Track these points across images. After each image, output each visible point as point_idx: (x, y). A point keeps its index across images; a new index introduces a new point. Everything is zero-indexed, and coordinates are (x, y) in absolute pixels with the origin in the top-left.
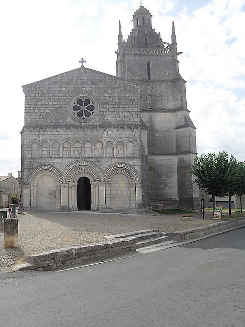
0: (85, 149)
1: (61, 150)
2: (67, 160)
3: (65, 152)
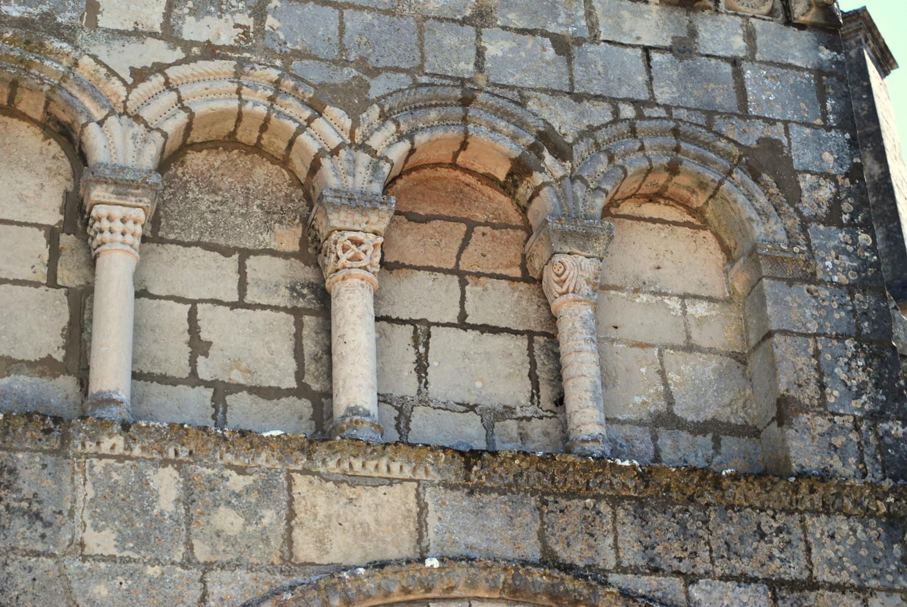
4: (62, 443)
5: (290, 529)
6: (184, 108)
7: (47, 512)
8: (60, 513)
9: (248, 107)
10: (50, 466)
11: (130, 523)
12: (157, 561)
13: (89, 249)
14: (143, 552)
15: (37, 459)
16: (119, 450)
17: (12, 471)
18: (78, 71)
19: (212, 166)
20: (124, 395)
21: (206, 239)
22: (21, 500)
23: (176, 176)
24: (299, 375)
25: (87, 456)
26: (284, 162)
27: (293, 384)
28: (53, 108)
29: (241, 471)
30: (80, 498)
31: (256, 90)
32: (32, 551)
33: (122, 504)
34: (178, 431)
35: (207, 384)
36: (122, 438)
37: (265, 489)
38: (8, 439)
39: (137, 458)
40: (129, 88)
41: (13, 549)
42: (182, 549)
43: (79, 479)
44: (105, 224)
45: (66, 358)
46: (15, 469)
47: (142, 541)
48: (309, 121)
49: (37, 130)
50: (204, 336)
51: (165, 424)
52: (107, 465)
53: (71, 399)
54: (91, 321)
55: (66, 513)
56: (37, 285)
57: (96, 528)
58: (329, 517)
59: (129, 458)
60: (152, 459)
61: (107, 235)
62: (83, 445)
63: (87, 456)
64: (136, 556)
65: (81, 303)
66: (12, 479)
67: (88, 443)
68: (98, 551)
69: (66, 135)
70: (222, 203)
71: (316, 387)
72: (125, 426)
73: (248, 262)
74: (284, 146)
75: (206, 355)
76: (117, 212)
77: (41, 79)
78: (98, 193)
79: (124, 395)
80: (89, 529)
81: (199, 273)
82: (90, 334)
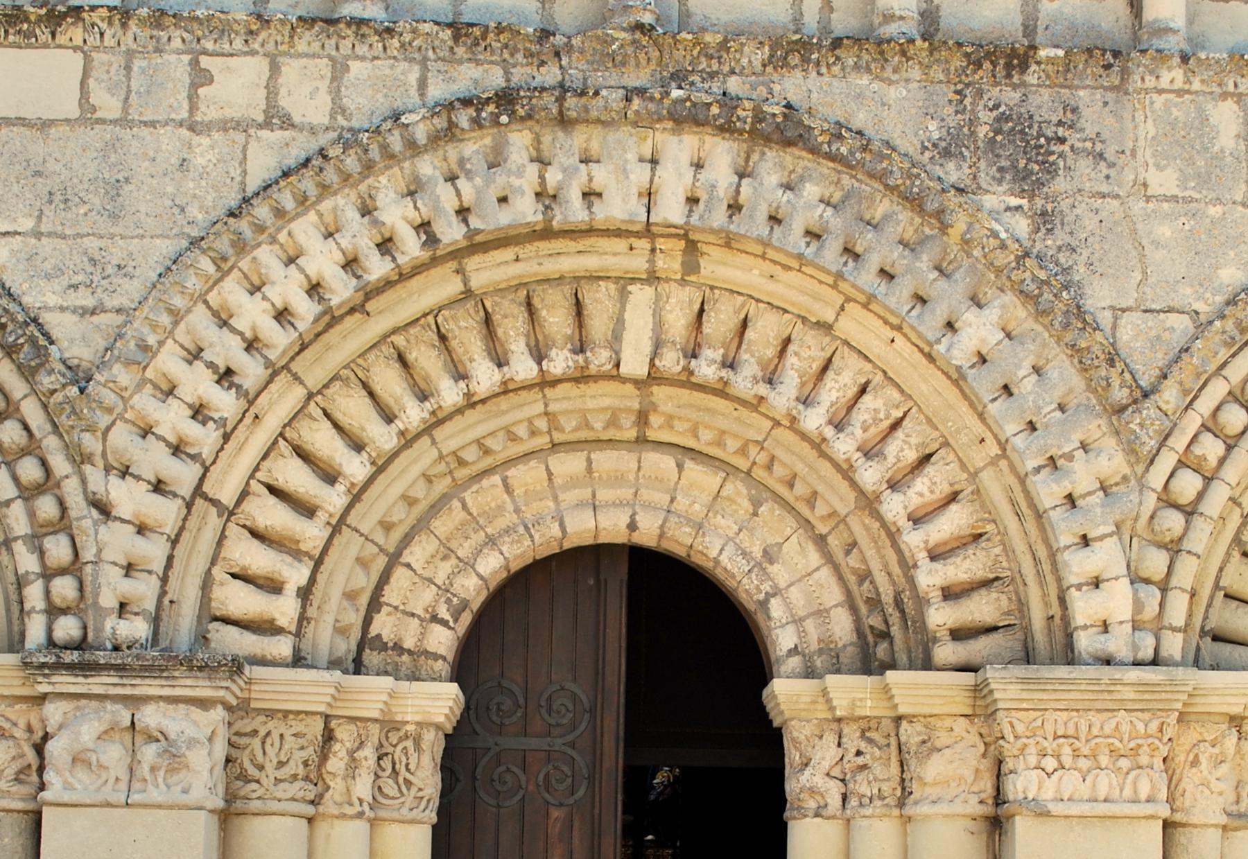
2: (237, 82)
4: (1122, 79)
7: (1110, 154)
8: (1123, 152)
10: (1111, 104)
11: (1190, 161)
12: (1219, 201)
14: (1204, 192)
15: (1099, 96)
16: (1179, 84)
17: (1074, 110)
20: (1179, 22)
22: (1085, 140)
25: (1147, 91)
32: (1098, 193)
33: (1183, 141)
36: (1181, 71)
38: (1069, 76)
39: (1197, 92)
41: (1079, 190)
43: (1139, 115)
46: (1078, 108)
47: (1204, 180)
51: (1225, 56)
52: (1166, 100)
55: (1128, 153)
57: (1158, 167)
59: (1188, 92)
60: (1212, 93)
62: (1143, 79)
63: (1147, 91)
64: (1197, 196)
66: (1075, 118)
67: (1147, 78)
68: (1161, 191)
72: (1185, 59)
79: (1179, 22)
80: (1152, 169)
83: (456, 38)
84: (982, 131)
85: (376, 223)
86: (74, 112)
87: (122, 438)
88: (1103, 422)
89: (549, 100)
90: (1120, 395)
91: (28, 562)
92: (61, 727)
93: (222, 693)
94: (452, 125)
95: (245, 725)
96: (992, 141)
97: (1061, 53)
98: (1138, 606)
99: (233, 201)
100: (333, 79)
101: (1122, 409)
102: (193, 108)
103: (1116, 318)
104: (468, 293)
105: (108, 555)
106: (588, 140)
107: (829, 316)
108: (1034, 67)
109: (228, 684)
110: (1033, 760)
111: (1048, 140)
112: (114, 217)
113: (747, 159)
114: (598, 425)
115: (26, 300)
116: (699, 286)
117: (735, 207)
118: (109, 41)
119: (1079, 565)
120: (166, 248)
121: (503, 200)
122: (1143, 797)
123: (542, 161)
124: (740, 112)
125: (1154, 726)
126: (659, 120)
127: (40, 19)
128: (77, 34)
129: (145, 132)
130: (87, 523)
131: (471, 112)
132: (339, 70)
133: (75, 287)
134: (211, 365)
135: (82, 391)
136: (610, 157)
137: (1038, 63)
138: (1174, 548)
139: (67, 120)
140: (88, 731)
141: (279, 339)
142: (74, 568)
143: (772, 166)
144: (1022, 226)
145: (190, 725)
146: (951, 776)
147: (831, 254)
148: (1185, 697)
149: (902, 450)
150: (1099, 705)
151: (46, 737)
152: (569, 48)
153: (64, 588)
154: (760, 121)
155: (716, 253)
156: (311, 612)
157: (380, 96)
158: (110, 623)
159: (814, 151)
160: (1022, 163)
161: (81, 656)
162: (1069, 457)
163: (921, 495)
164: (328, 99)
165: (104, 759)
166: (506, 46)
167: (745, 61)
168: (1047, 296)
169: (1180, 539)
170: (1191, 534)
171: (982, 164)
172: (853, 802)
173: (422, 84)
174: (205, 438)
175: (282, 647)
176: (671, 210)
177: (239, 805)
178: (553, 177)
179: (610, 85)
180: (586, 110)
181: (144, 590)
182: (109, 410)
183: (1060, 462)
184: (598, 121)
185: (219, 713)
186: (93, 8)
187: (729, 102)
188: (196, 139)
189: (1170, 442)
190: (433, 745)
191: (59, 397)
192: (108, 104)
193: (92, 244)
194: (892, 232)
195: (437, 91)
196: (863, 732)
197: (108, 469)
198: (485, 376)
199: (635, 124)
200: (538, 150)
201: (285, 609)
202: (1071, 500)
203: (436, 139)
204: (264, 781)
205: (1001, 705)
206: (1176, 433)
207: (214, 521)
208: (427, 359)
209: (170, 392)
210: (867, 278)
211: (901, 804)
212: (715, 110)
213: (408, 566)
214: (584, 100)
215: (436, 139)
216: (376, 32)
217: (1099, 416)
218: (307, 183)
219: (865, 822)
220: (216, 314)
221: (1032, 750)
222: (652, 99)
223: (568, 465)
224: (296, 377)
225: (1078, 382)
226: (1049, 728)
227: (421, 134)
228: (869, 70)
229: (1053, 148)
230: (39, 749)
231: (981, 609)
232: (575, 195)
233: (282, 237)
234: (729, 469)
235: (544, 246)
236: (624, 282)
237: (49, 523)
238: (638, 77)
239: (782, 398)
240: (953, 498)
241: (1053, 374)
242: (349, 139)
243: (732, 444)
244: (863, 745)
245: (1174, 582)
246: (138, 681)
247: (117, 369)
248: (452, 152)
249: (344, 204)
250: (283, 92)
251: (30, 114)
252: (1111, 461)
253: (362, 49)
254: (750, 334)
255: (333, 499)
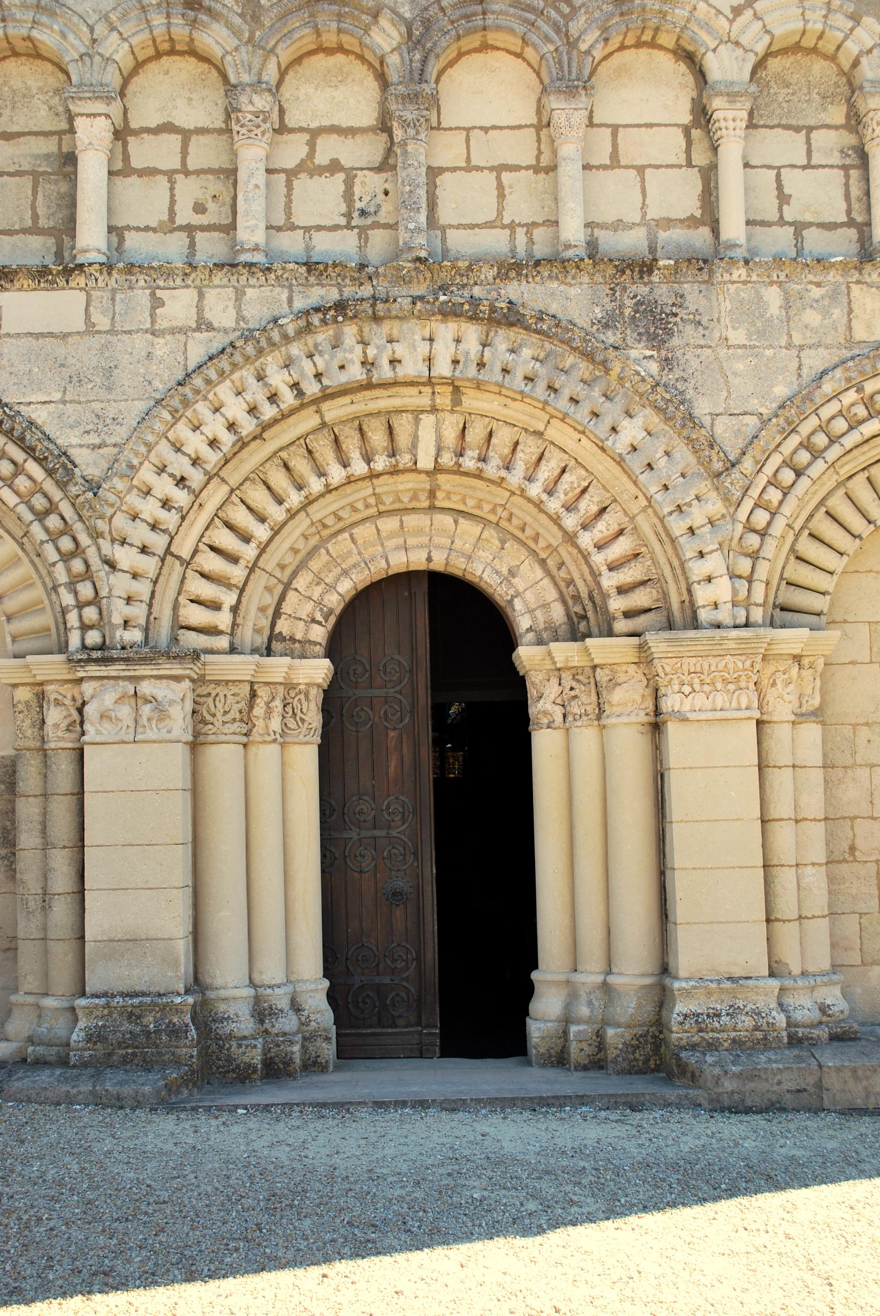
0: (448, 150)
1: (92, 169)
2: (179, 305)
3: (145, 202)
5: (850, 321)
6: (767, 32)
7: (704, 322)
9: (810, 26)
11: (753, 323)
13: (711, 139)
17: (682, 296)
18: (696, 14)
19: (785, 68)
20: (742, 241)
21: (784, 122)
23: (761, 78)
24: (849, 212)
26: (833, 58)
27: (845, 219)
28: (681, 42)
29: (818, 285)
30: (723, 309)
31: (815, 11)
34: (778, 260)
35: (790, 224)
37: (833, 296)
40: (731, 22)
42: (785, 337)
43: (721, 298)
44: (723, 124)
45: (702, 215)
47: (761, 334)
48: (852, 30)
49: (670, 56)
50: (787, 191)
53: (708, 242)
54: (717, 188)
56: (680, 167)
57: (734, 328)
58: (873, 311)
59: (749, 282)
61: (724, 131)
65: (709, 177)
69: (690, 59)
70: (793, 94)
71: (859, 219)
72: (747, 262)
73: (812, 136)
74: (833, 48)
75: (788, 204)
76: (730, 114)
77: (674, 23)
78: (717, 103)
79: (742, 241)
80: (730, 329)
81: (783, 147)
82: (717, 197)
83: (309, 271)
84: (627, 312)
85: (267, 385)
86: (82, 328)
87: (121, 522)
88: (708, 483)
89: (366, 306)
90: (718, 466)
91: (68, 599)
92: (92, 697)
93: (188, 672)
94: (309, 324)
95: (203, 690)
96: (634, 317)
97: (672, 262)
98: (735, 592)
99: (180, 376)
100: (237, 300)
101: (719, 474)
102: (153, 322)
103: (713, 420)
104: (324, 424)
105: (115, 592)
106: (391, 329)
107: (541, 427)
108: (656, 272)
109: (192, 666)
110: (676, 688)
111: (667, 315)
112: (109, 389)
113: (487, 336)
114: (406, 500)
115: (59, 442)
116: (462, 413)
117: (481, 365)
118: (101, 284)
119: (698, 569)
120: (141, 406)
121: (342, 367)
122: (744, 706)
123: (364, 343)
124: (481, 308)
125: (748, 664)
126: (433, 315)
127: (59, 272)
128: (81, 280)
129: (125, 337)
130: (102, 574)
131: (320, 315)
132: (240, 294)
133: (88, 432)
134: (172, 475)
135: (95, 494)
136: (405, 338)
137: (659, 269)
138: (755, 556)
139: (78, 333)
140: (109, 699)
141: (212, 458)
142: (96, 601)
143: (502, 339)
144: (654, 367)
145: (172, 693)
146: (628, 700)
147: (540, 390)
148: (765, 645)
149: (588, 505)
150: (715, 653)
151: (84, 704)
152: (377, 274)
153: (90, 613)
154: (494, 312)
155: (471, 393)
156: (239, 620)
157: (265, 309)
158: (119, 633)
159: (527, 328)
160: (652, 330)
161: (102, 654)
162: (689, 505)
163: (601, 532)
164: (234, 312)
165: (119, 715)
166: (339, 275)
167: (482, 277)
168: (671, 409)
169: (758, 551)
170: (764, 547)
171: (628, 332)
172: (570, 718)
173: (290, 300)
174: (170, 519)
175: (223, 642)
176: (443, 368)
177: (202, 738)
178: (371, 352)
179: (403, 294)
180: (389, 310)
181: (138, 612)
182: (112, 505)
183: (684, 508)
184: (397, 317)
185: (187, 684)
186: (90, 265)
187: (474, 301)
188: (156, 340)
189: (749, 493)
190: (316, 696)
191: (81, 499)
192: (102, 322)
193: (97, 406)
194: (576, 375)
195: (299, 304)
196: (574, 676)
197: (113, 541)
198: (337, 474)
199: (419, 318)
200: (361, 336)
201: (223, 620)
202: (691, 530)
203: (300, 333)
204: (216, 723)
205: (655, 656)
206: (753, 487)
207: (178, 568)
208: (301, 465)
209: (148, 492)
210: (563, 403)
211: (599, 718)
212: (466, 307)
213: (296, 590)
214: (387, 305)
215: (300, 333)
216: (261, 270)
217: (705, 479)
218: (224, 363)
219: (578, 730)
220: (173, 444)
221: (676, 681)
222: (428, 302)
223: (389, 524)
224: (223, 480)
225: (692, 459)
226: (685, 669)
227: (291, 330)
228: (557, 278)
229: (670, 320)
230: (80, 711)
231: (641, 598)
232: (385, 362)
233: (211, 396)
234: (486, 522)
235: (368, 394)
236: (417, 413)
237: (80, 575)
238: (419, 290)
239: (515, 478)
240: (621, 532)
241: (677, 455)
242: (248, 336)
243: (487, 507)
244: (574, 684)
245: (756, 577)
246: (137, 667)
247: (116, 480)
248: (310, 340)
249: (247, 375)
250: (207, 309)
251: (56, 329)
252: (714, 506)
253: (253, 281)
254: (494, 440)
255: (249, 552)
